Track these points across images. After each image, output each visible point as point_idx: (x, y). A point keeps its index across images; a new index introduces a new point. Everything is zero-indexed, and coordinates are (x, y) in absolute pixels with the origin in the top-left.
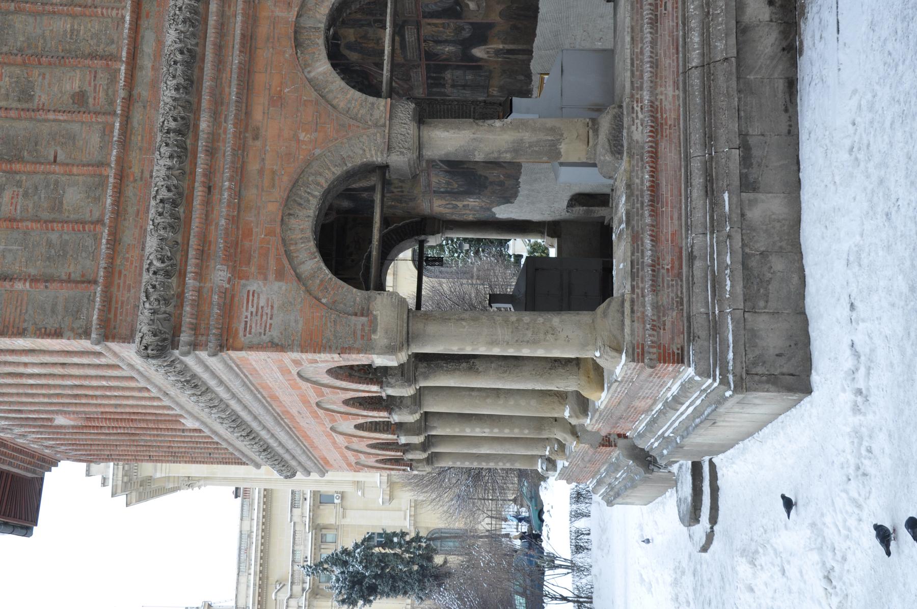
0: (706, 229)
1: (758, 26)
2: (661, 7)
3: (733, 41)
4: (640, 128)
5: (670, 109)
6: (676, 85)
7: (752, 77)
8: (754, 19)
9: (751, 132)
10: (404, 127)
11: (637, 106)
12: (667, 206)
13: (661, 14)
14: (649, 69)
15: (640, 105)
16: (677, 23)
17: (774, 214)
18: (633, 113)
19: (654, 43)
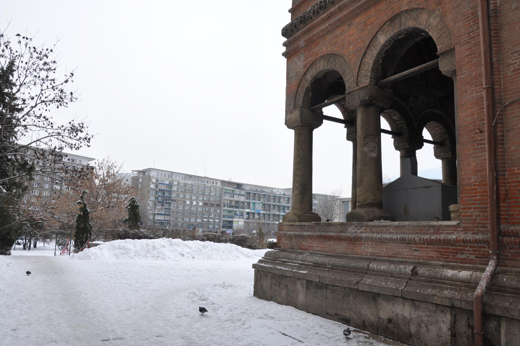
0: (303, 262)
1: (377, 308)
2: (416, 247)
3: (366, 289)
4: (353, 231)
5: (360, 250)
6: (372, 254)
7: (351, 298)
8: (380, 306)
9: (328, 291)
10: (358, 97)
11: (363, 230)
12: (322, 244)
13: (412, 247)
14: (377, 237)
15: (364, 231)
16: (405, 258)
17: (299, 295)
18: (360, 227)
19: (392, 240)
